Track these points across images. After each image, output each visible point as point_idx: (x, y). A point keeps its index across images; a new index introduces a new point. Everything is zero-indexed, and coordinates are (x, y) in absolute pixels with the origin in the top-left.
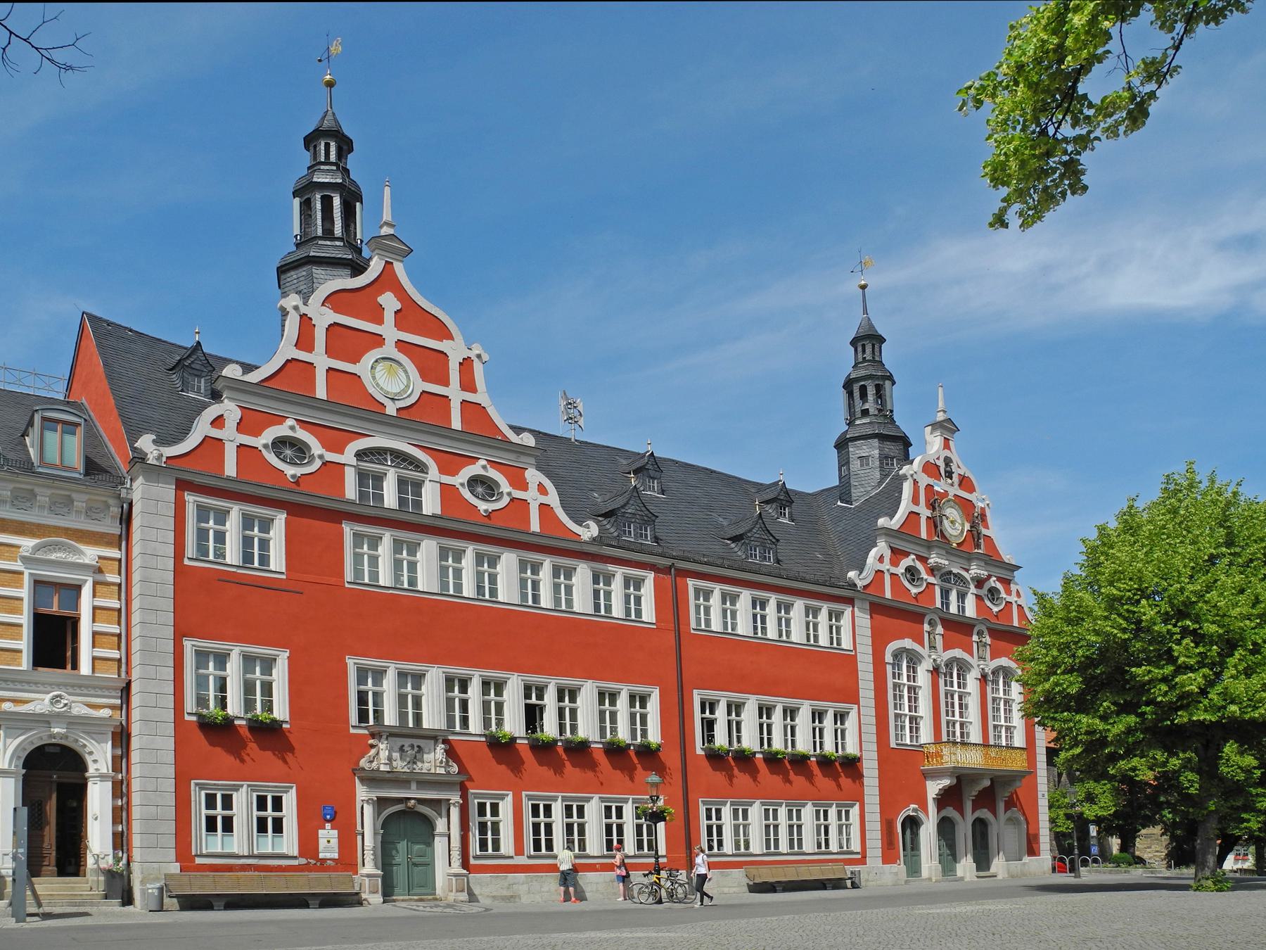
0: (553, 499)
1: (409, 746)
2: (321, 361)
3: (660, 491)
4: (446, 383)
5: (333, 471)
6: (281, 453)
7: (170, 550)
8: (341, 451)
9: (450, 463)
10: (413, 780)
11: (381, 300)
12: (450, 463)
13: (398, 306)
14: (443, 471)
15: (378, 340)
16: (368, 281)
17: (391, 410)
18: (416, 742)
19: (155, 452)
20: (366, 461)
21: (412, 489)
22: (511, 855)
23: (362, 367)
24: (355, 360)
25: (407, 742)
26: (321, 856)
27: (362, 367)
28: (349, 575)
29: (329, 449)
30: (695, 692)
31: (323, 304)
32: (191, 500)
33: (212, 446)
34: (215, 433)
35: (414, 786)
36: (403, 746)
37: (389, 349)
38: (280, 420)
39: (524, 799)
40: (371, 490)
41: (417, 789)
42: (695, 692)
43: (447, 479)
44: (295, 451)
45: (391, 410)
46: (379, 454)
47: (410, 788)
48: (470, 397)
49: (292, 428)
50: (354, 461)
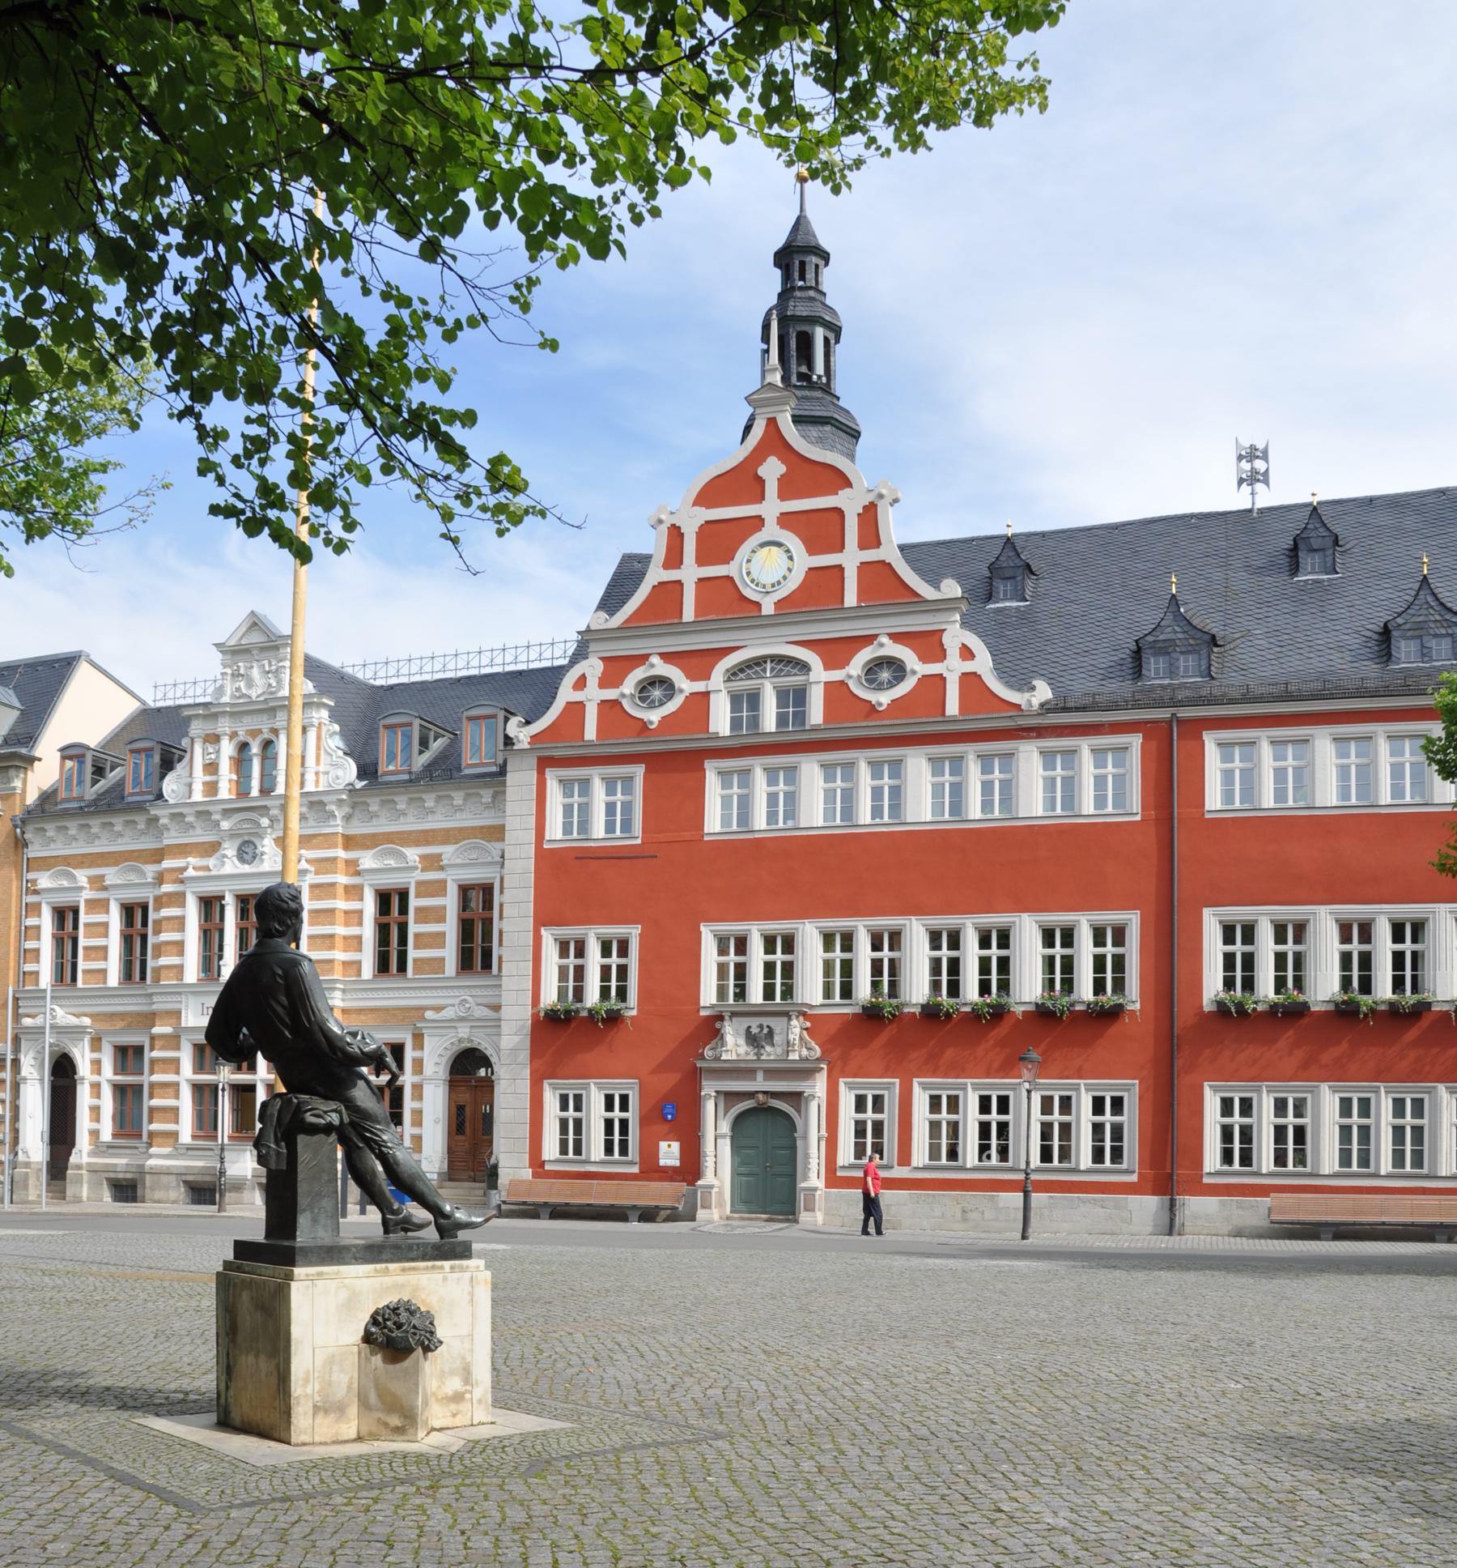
0: (983, 663)
7: (531, 836)
9: (836, 651)
12: (836, 651)
13: (782, 469)
14: (828, 666)
15: (758, 522)
17: (768, 609)
18: (766, 1021)
20: (741, 679)
21: (793, 699)
24: (727, 557)
25: (754, 1023)
26: (662, 1162)
29: (692, 676)
30: (1207, 913)
31: (696, 503)
34: (578, 696)
35: (760, 1076)
36: (749, 1027)
37: (771, 530)
38: (642, 659)
39: (842, 1088)
42: (1207, 913)
43: (836, 675)
44: (665, 690)
45: (768, 609)
46: (758, 664)
48: (871, 555)
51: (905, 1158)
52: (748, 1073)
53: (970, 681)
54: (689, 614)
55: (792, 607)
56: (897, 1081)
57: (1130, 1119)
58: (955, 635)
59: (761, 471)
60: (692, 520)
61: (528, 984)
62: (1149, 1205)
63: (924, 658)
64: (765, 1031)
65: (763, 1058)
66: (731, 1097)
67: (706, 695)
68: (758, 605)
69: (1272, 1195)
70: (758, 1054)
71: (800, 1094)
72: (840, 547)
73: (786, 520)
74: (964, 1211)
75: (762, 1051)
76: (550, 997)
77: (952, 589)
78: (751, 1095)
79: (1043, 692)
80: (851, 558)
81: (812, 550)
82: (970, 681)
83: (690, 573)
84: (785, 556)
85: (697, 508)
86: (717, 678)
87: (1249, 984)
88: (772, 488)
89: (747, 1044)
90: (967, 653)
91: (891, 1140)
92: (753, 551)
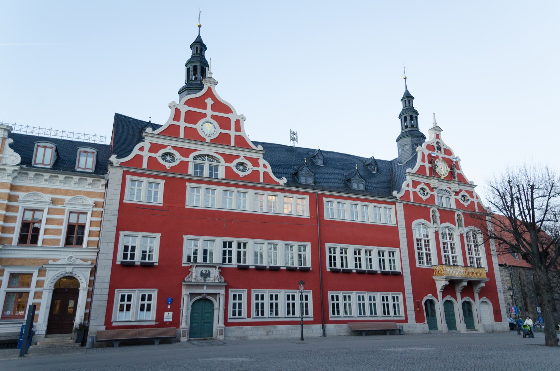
1: (205, 271)
2: (182, 124)
3: (323, 164)
4: (229, 129)
6: (165, 159)
10: (205, 285)
15: (204, 116)
16: (202, 94)
18: (208, 269)
19: (116, 161)
20: (198, 160)
22: (245, 317)
23: (198, 126)
24: (195, 123)
27: (198, 126)
32: (128, 178)
33: (139, 158)
35: (205, 287)
36: (202, 271)
40: (199, 171)
41: (207, 289)
45: (208, 140)
46: (203, 157)
47: (203, 289)
49: (170, 149)
50: (192, 160)
52: (198, 285)
60: (184, 109)
64: (207, 272)
65: (206, 281)
66: (192, 295)
68: (205, 139)
70: (205, 280)
75: (206, 279)
84: (213, 127)
85: (184, 105)
86: (190, 159)
88: (209, 107)
92: (203, 123)
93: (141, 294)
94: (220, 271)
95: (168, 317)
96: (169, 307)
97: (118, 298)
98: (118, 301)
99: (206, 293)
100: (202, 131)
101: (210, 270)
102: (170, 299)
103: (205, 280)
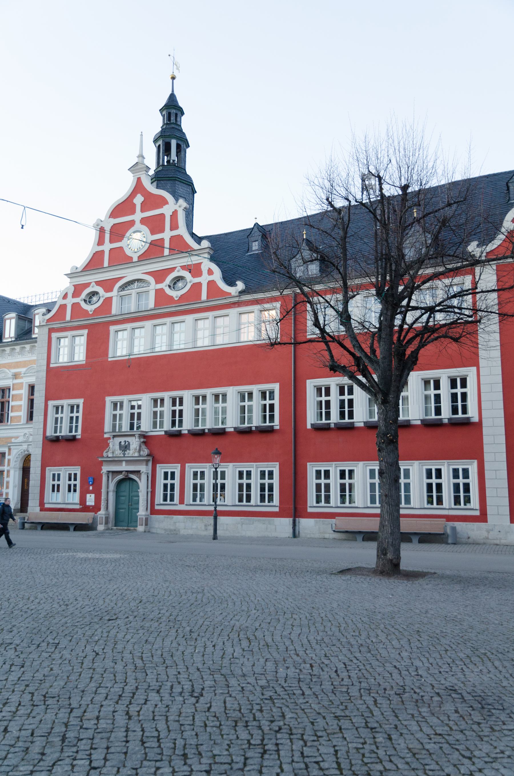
5: (108, 301)
8: (111, 290)
11: (135, 201)
13: (142, 199)
14: (157, 283)
17: (135, 259)
25: (122, 440)
26: (88, 504)
28: (110, 355)
30: (308, 381)
31: (110, 217)
35: (124, 463)
36: (120, 442)
37: (138, 225)
42: (308, 381)
43: (159, 286)
45: (135, 259)
47: (122, 465)
48: (175, 233)
51: (182, 501)
53: (211, 284)
54: (106, 264)
55: (145, 257)
56: (179, 465)
57: (276, 481)
58: (207, 264)
59: (135, 201)
61: (42, 426)
62: (286, 522)
63: (194, 276)
67: (111, 298)
68: (131, 258)
69: (336, 518)
70: (124, 454)
71: (139, 471)
72: (162, 231)
73: (143, 221)
74: (205, 526)
76: (50, 433)
77: (205, 244)
78: (120, 472)
79: (240, 285)
80: (167, 235)
81: (153, 233)
82: (211, 284)
83: (107, 247)
85: (111, 219)
87: (328, 415)
89: (120, 449)
90: (210, 272)
91: (177, 493)
93: (68, 473)
94: (142, 440)
95: (90, 499)
96: (91, 488)
97: (50, 477)
98: (50, 481)
99: (126, 471)
100: (129, 247)
101: (130, 441)
102: (91, 479)
103: (124, 454)
